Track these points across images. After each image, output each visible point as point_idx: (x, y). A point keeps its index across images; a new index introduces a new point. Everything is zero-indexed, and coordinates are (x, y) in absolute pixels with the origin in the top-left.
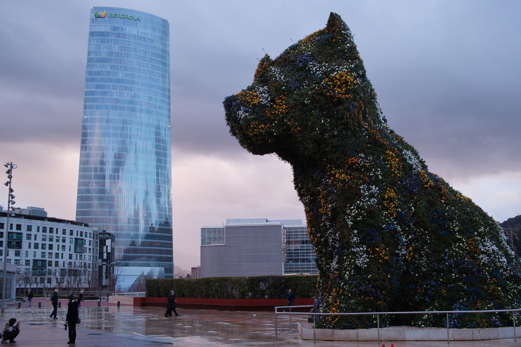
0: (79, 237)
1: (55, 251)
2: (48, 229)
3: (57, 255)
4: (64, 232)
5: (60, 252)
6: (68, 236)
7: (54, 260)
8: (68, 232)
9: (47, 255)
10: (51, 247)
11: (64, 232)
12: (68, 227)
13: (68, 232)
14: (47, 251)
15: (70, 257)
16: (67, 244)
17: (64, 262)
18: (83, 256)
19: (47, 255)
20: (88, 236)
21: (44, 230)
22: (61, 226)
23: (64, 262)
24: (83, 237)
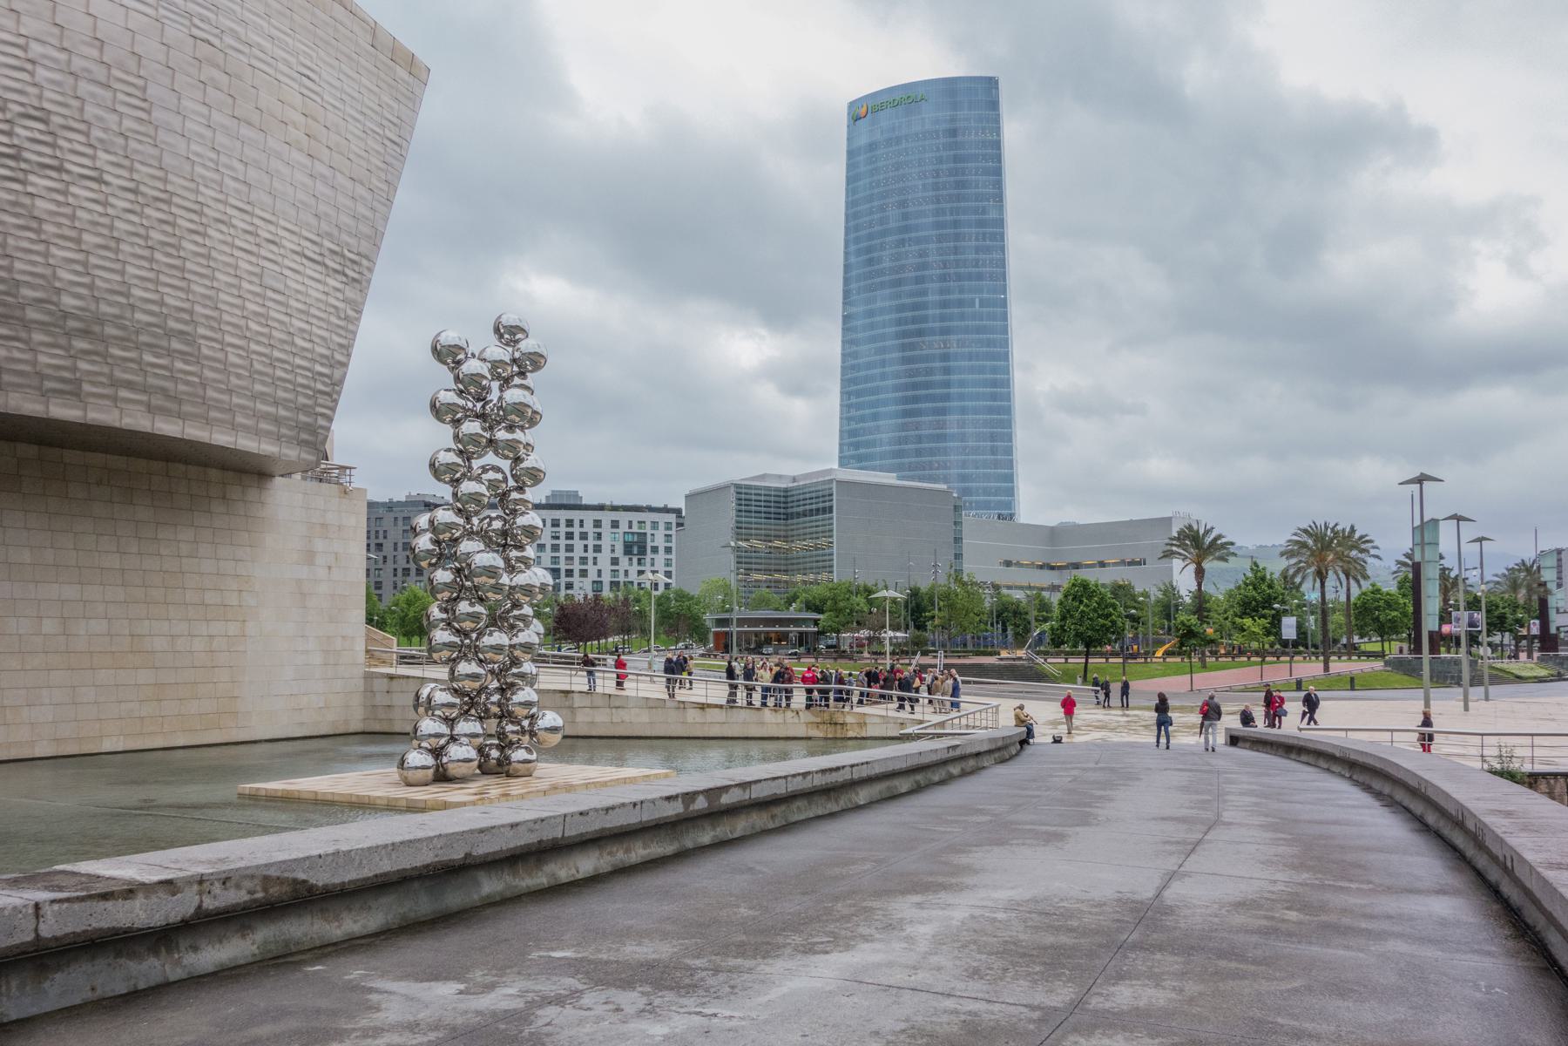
0: (635, 529)
1: (578, 552)
2: (563, 523)
3: (584, 560)
4: (597, 524)
5: (590, 554)
6: (606, 529)
7: (577, 567)
8: (606, 524)
9: (562, 561)
10: (570, 548)
11: (597, 524)
12: (606, 517)
13: (606, 524)
14: (562, 554)
15: (615, 561)
16: (606, 543)
17: (599, 571)
18: (648, 560)
19: (562, 561)
20: (662, 526)
21: (555, 524)
22: (589, 517)
23: (599, 571)
24: (648, 531)
